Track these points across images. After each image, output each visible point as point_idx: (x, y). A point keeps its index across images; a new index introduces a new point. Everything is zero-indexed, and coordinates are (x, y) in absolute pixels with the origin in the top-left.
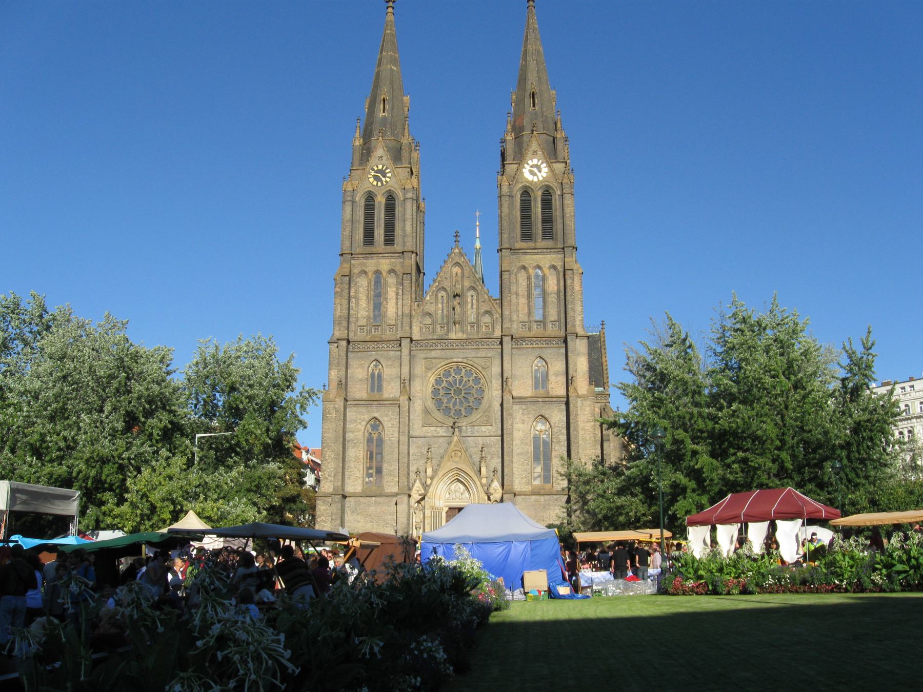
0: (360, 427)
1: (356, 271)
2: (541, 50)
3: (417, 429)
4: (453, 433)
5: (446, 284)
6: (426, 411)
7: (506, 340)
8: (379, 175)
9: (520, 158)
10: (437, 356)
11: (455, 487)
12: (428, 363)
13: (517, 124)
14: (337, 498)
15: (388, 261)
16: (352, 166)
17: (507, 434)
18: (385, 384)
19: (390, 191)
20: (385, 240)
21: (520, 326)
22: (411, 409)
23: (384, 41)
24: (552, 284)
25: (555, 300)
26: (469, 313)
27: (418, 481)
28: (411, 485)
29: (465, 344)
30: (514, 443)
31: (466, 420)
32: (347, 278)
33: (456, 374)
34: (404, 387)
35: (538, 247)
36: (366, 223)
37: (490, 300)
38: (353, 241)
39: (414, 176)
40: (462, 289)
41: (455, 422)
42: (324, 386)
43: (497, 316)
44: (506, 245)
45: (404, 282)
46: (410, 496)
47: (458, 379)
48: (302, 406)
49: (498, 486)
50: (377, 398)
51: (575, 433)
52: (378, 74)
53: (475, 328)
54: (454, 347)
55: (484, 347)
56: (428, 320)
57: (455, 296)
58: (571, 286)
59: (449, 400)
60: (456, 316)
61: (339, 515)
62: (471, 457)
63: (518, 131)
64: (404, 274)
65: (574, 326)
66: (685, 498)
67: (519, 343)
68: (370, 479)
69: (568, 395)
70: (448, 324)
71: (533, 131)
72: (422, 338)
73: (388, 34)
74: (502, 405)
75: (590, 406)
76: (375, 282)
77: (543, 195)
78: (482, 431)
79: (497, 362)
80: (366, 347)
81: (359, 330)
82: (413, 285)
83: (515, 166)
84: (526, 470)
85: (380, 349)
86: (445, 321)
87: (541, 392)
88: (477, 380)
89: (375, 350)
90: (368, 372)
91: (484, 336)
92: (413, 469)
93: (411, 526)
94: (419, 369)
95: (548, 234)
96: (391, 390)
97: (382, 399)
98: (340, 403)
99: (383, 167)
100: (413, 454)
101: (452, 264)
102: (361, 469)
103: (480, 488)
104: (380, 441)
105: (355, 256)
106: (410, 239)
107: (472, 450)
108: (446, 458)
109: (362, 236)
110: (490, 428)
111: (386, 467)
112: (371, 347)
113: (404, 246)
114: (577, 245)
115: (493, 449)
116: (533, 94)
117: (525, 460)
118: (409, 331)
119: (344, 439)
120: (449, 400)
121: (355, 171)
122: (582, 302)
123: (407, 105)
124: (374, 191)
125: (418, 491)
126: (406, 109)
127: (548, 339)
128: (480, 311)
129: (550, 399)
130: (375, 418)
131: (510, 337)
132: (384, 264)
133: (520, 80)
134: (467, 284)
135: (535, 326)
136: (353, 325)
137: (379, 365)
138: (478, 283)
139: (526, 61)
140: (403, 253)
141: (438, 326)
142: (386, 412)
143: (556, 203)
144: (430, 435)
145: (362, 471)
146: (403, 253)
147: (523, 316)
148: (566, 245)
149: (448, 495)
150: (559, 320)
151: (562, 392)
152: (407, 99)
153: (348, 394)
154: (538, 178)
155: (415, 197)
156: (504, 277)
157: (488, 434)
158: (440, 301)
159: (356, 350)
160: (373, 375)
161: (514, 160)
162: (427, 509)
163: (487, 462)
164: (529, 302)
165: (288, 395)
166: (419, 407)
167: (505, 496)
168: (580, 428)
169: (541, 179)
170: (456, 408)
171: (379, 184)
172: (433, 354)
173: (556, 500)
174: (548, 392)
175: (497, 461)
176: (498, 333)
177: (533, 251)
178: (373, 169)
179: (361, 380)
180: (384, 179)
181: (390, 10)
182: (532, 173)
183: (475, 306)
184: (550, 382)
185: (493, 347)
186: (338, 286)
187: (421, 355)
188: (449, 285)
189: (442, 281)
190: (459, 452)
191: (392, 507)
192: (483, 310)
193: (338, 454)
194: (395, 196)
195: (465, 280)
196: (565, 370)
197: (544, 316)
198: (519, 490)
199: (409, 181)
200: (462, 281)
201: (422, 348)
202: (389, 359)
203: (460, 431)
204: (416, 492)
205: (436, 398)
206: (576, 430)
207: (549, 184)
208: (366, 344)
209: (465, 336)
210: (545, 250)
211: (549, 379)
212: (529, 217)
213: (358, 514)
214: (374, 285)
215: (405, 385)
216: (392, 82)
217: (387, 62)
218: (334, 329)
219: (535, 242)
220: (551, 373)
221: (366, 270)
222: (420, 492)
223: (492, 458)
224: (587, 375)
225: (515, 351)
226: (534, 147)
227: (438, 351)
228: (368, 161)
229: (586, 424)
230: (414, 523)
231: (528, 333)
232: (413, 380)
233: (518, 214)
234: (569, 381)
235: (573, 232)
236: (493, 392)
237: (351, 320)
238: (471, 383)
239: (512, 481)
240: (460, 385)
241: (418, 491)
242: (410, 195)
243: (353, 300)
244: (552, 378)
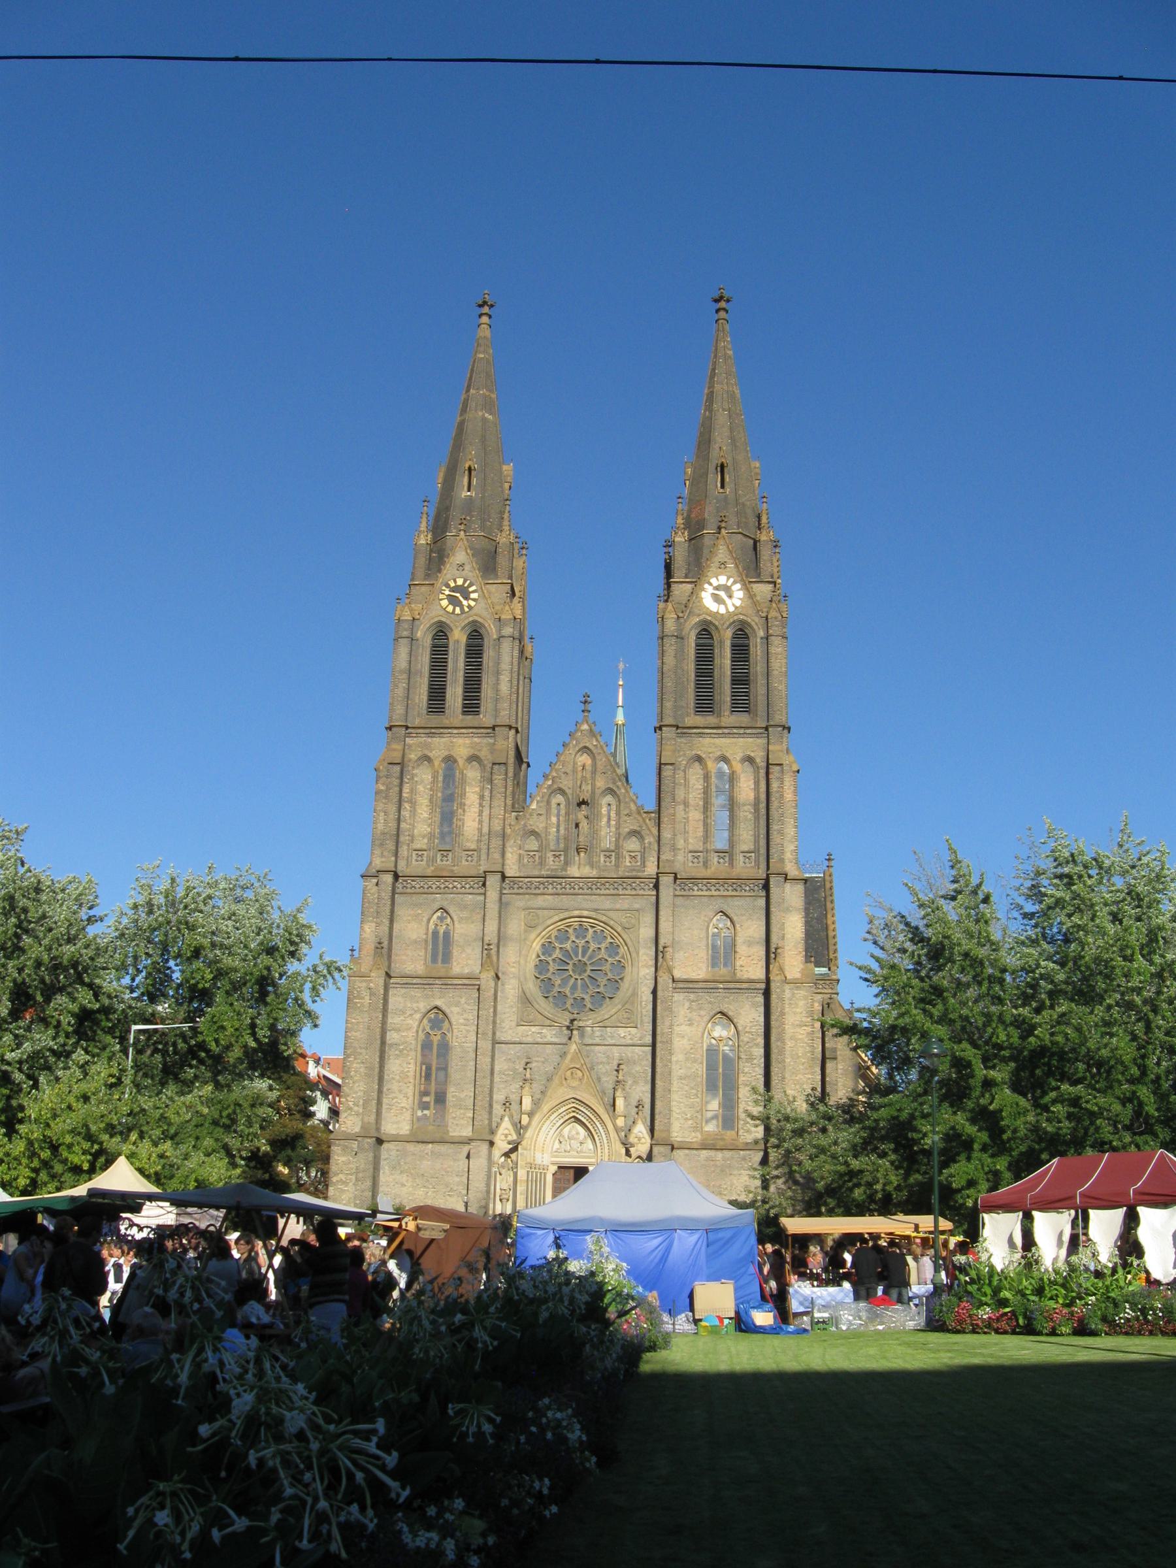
0: (411, 1022)
1: (413, 756)
2: (737, 392)
3: (509, 1029)
4: (570, 1039)
5: (566, 783)
6: (525, 1000)
7: (666, 880)
8: (458, 595)
9: (697, 574)
10: (544, 905)
11: (570, 1132)
13: (693, 515)
14: (368, 1143)
15: (468, 741)
16: (412, 580)
17: (661, 1042)
18: (455, 952)
19: (474, 622)
20: (465, 706)
21: (690, 858)
22: (499, 994)
23: (472, 370)
24: (746, 788)
25: (750, 816)
26: (603, 833)
27: (506, 1119)
28: (494, 1125)
29: (594, 887)
30: (674, 1059)
31: (592, 1015)
32: (398, 768)
33: (577, 937)
34: (489, 956)
35: (723, 724)
36: (432, 675)
37: (639, 813)
38: (410, 706)
39: (516, 599)
40: (593, 792)
41: (574, 1020)
42: (352, 950)
43: (650, 839)
44: (668, 720)
45: (495, 777)
46: (492, 1144)
47: (580, 945)
48: (314, 988)
49: (644, 1131)
50: (441, 974)
51: (779, 1043)
52: (461, 426)
53: (613, 858)
54: (576, 891)
55: (627, 892)
56: (533, 844)
57: (580, 804)
58: (778, 792)
59: (565, 981)
60: (581, 839)
61: (370, 1173)
62: (599, 1079)
63: (695, 528)
64: (494, 764)
65: (782, 861)
66: (969, 1159)
67: (687, 888)
68: (426, 1112)
69: (768, 981)
70: (566, 850)
71: (719, 528)
72: (522, 875)
73: (482, 358)
74: (654, 992)
75: (805, 998)
76: (445, 777)
77: (735, 636)
78: (619, 1035)
79: (649, 918)
80: (426, 886)
81: (414, 857)
82: (510, 783)
83: (689, 586)
84: (692, 1106)
85: (451, 891)
86: (562, 846)
87: (723, 971)
88: (613, 949)
89: (442, 891)
90: (428, 929)
92: (499, 1097)
93: (492, 1196)
94: (515, 926)
95: (741, 703)
96: (466, 960)
97: (450, 975)
98: (378, 980)
99: (465, 581)
100: (500, 1072)
102: (410, 1094)
103: (613, 1134)
104: (444, 1048)
105: (412, 731)
106: (506, 705)
107: (602, 1069)
108: (556, 1080)
109: (425, 698)
110: (633, 1031)
111: (452, 1093)
112: (434, 886)
113: (496, 717)
114: (790, 724)
115: (638, 1068)
116: (722, 466)
117: (693, 1088)
118: (501, 861)
119: (383, 1042)
120: (565, 981)
121: (418, 587)
122: (795, 819)
123: (509, 479)
124: (448, 622)
125: (506, 1136)
126: (507, 486)
127: (736, 882)
129: (738, 985)
130: (436, 1007)
131: (671, 877)
132: (462, 746)
133: (700, 442)
134: (601, 783)
135: (716, 859)
136: (405, 847)
137: (446, 918)
138: (619, 784)
139: (711, 411)
140: (493, 728)
141: (550, 854)
143: (756, 650)
144: (529, 1039)
145: (411, 1098)
146: (494, 729)
147: (695, 842)
148: (772, 723)
149: (557, 1145)
150: (756, 851)
151: (760, 974)
152: (508, 469)
153: (393, 965)
154: (727, 609)
155: (517, 635)
156: (664, 774)
157: (630, 1042)
158: (554, 811)
159: (409, 890)
160: (435, 934)
161: (686, 577)
162: (522, 1168)
163: (627, 1088)
164: (706, 817)
165: (293, 966)
166: (512, 991)
167: (656, 1150)
168: (787, 1036)
169: (731, 609)
170: (576, 995)
171: (458, 610)
172: (540, 901)
173: (744, 1159)
174: (735, 974)
176: (651, 869)
177: (715, 731)
178: (448, 586)
179: (415, 942)
180: (465, 603)
181: (485, 319)
182: (717, 599)
183: (613, 823)
184: (738, 956)
185: (642, 892)
186: (381, 781)
187: (520, 902)
188: (571, 786)
190: (579, 1074)
191: (461, 1163)
192: (627, 830)
193: (371, 1069)
194: (482, 631)
196: (764, 937)
197: (732, 842)
198: (679, 1139)
199: (507, 608)
200: (593, 779)
201: (521, 891)
202: (464, 907)
203: (582, 1036)
204: (503, 1137)
205: (542, 977)
206: (781, 1039)
207: (745, 618)
208: (426, 880)
209: (594, 873)
210: (735, 731)
211: (738, 950)
212: (710, 674)
213: (401, 1172)
214: (444, 781)
215: (490, 952)
216: (483, 440)
217: (476, 406)
218: (372, 854)
219: (719, 716)
220: (739, 940)
221: (429, 754)
222: (510, 1138)
223: (635, 1082)
224: (801, 947)
225: (679, 901)
226: (720, 556)
228: (440, 571)
229: (798, 1030)
230: (498, 1190)
231: (704, 870)
232: (504, 945)
233: (690, 667)
234: (770, 954)
235: (784, 700)
236: (641, 971)
237: (402, 839)
238: (603, 954)
239: (669, 1124)
240: (583, 956)
241: (506, 1136)
242: (508, 631)
243: (407, 805)
244: (742, 949)
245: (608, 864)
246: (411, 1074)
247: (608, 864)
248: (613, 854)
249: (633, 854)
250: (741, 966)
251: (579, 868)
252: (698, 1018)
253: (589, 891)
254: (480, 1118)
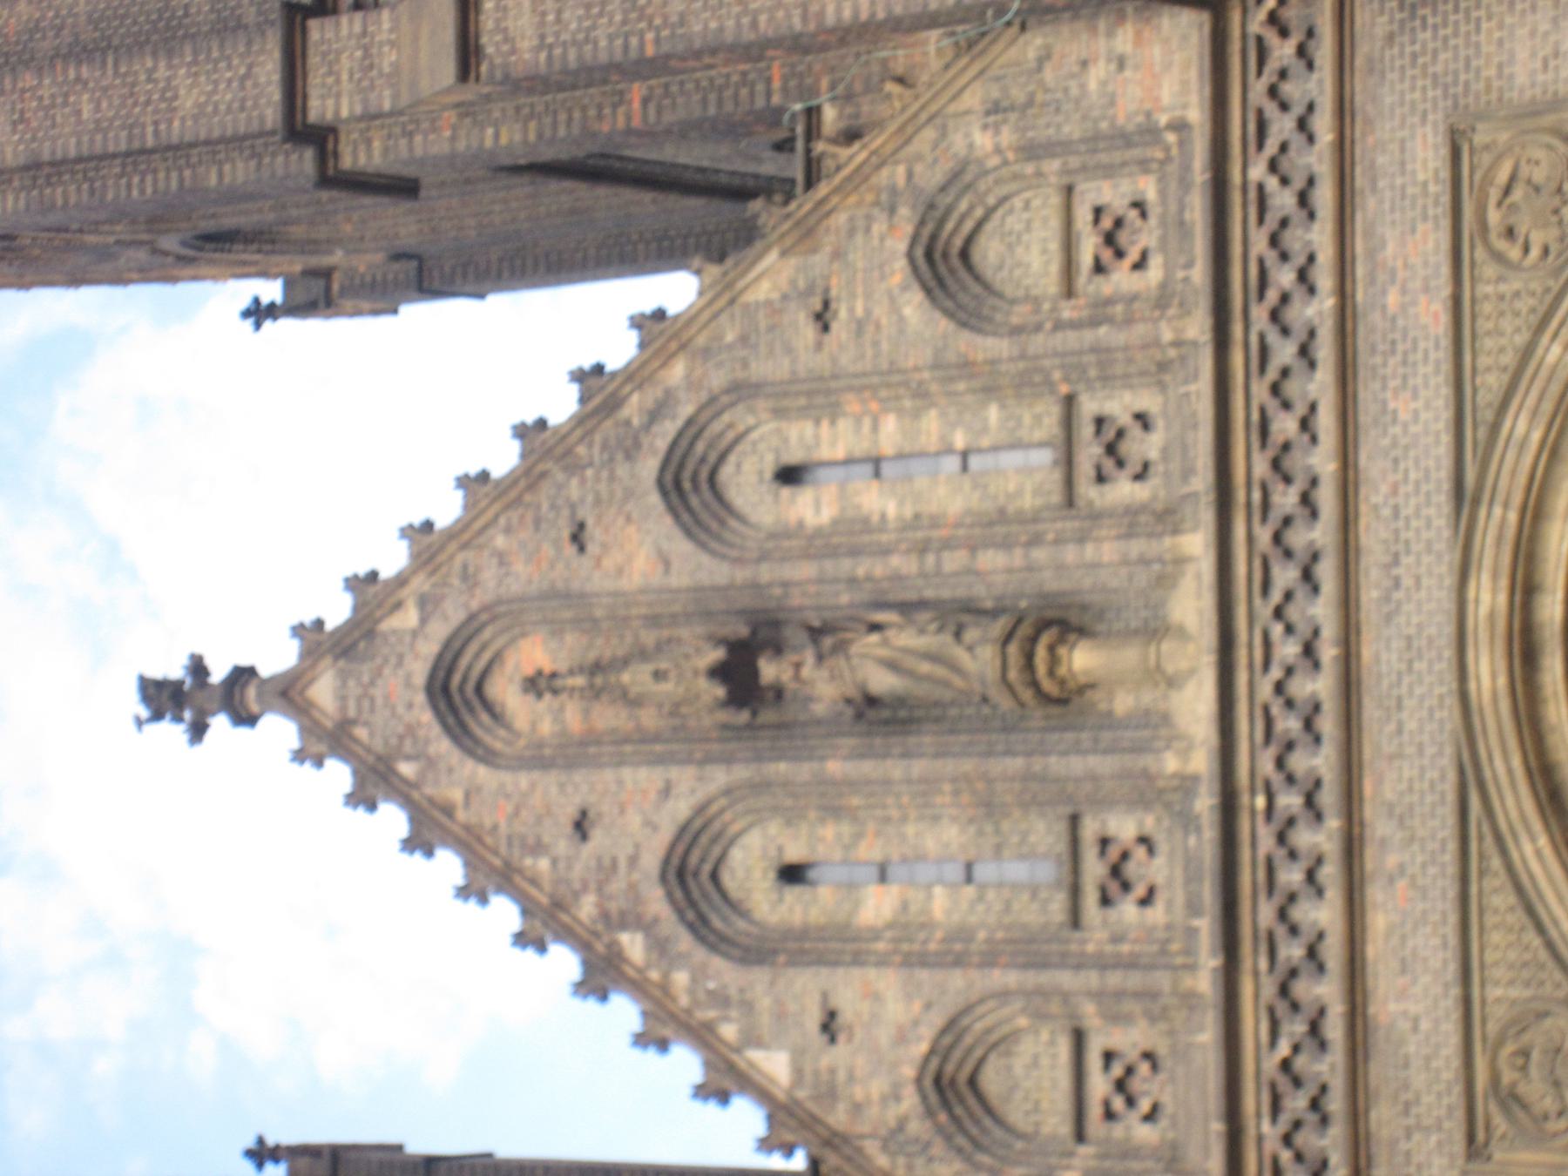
12: (1535, 1089)
91: (1199, 274)
101: (442, 746)
128: (916, 357)
138: (634, 407)
183: (890, 433)
189: (608, 869)
192: (914, 305)
195: (599, 582)
209: (1197, 543)
227: (1378, 922)
245: (1148, 446)
247: (1148, 446)
248: (1089, 407)
249: (1089, 247)
251: (1173, 682)
253: (1327, 572)
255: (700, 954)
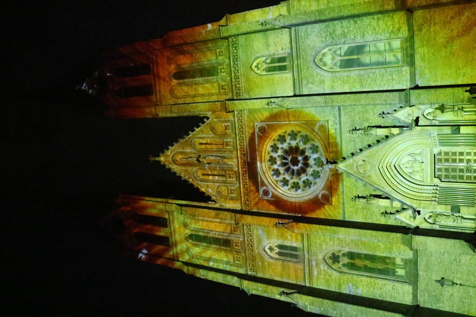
0: (333, 276)
51: (327, 13)
84: (382, 76)
92: (383, 221)
129: (294, 50)
130: (324, 259)
142: (317, 245)
157: (338, 125)
162: (435, 208)
175: (371, 114)
179: (284, 268)
184: (276, 52)
220: (266, 53)
223: (367, 120)
241: (410, 217)
243: (211, 264)
244: (272, 50)
246: (369, 280)
250: (282, 49)
252: (318, 77)
254: (395, 239)
255: (197, 181)
